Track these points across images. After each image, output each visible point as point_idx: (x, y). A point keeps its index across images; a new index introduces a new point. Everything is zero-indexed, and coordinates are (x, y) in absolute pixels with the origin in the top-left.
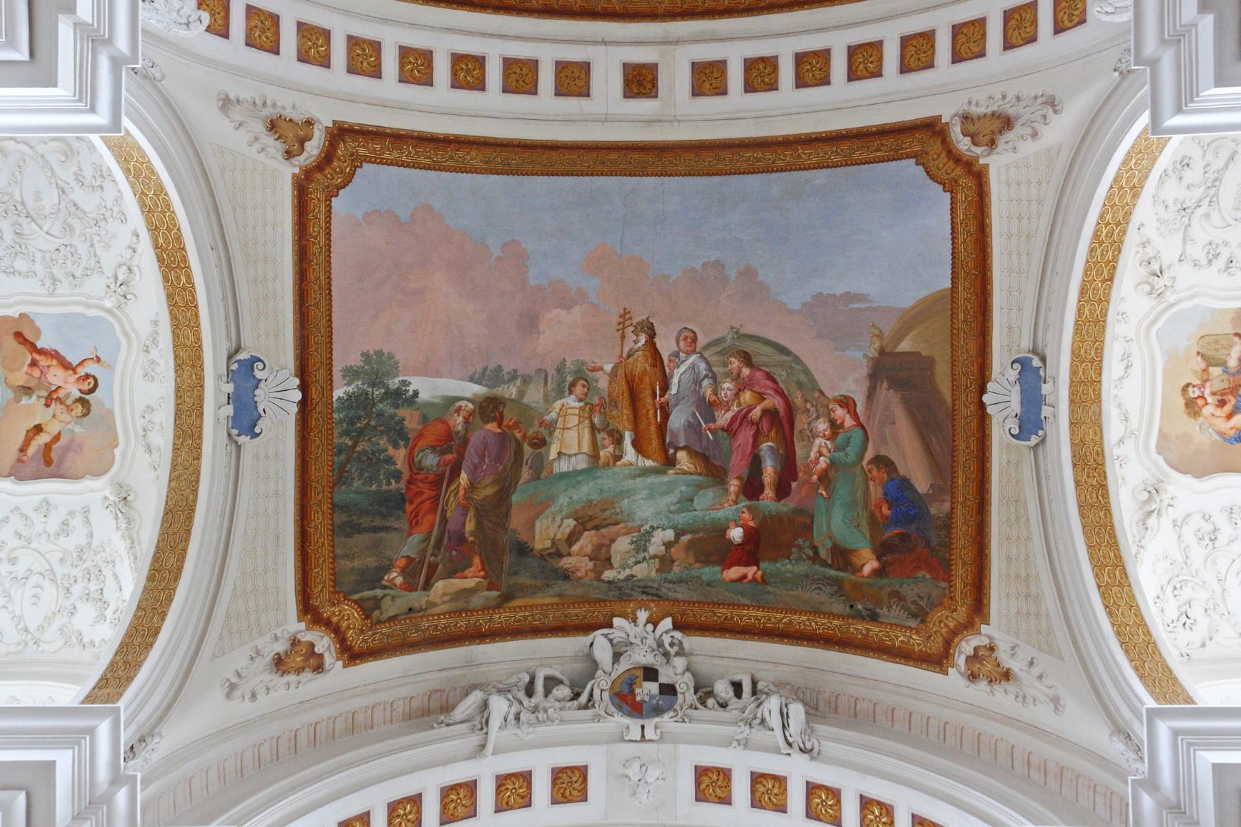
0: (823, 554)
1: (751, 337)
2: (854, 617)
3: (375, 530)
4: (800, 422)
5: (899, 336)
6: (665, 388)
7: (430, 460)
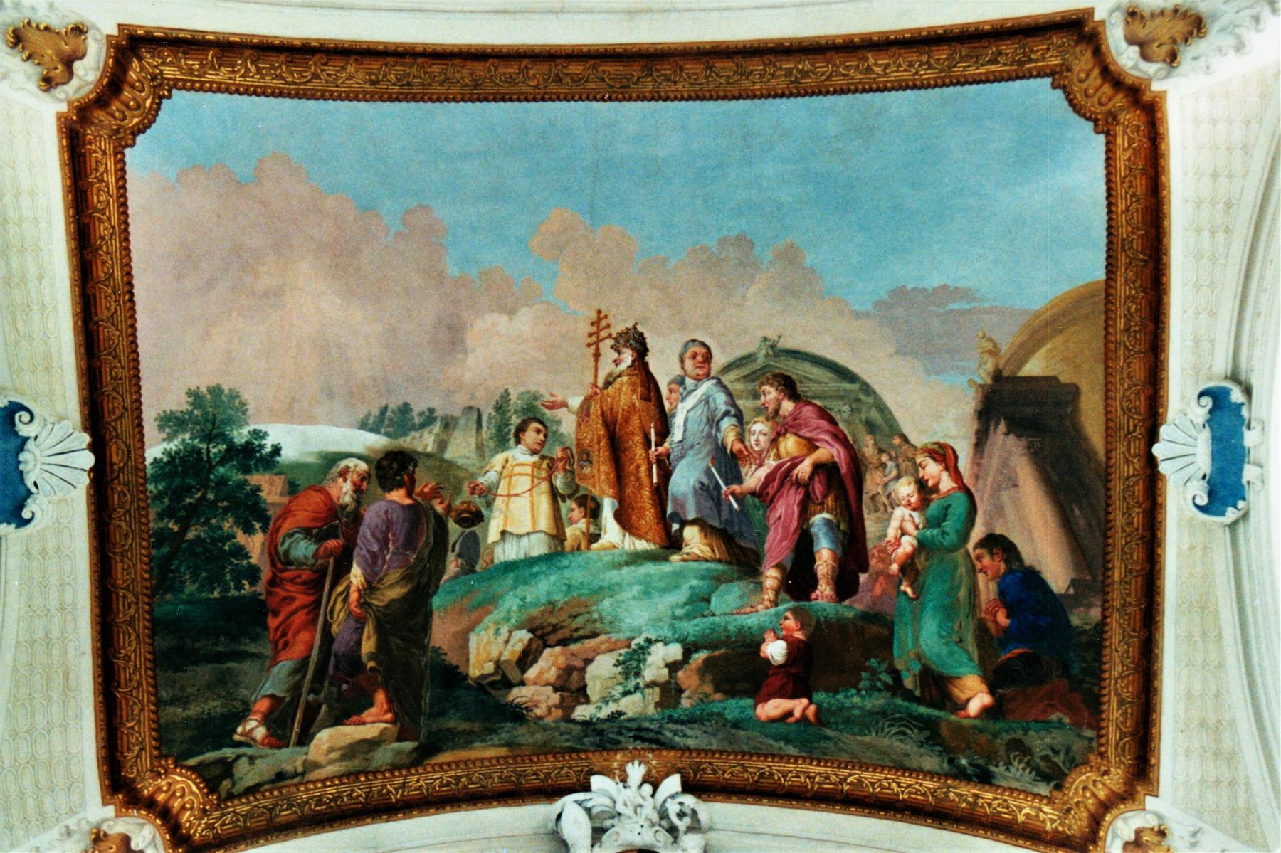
0: (908, 682)
1: (795, 354)
2: (955, 777)
3: (219, 658)
4: (873, 482)
5: (1026, 350)
6: (664, 432)
7: (303, 549)
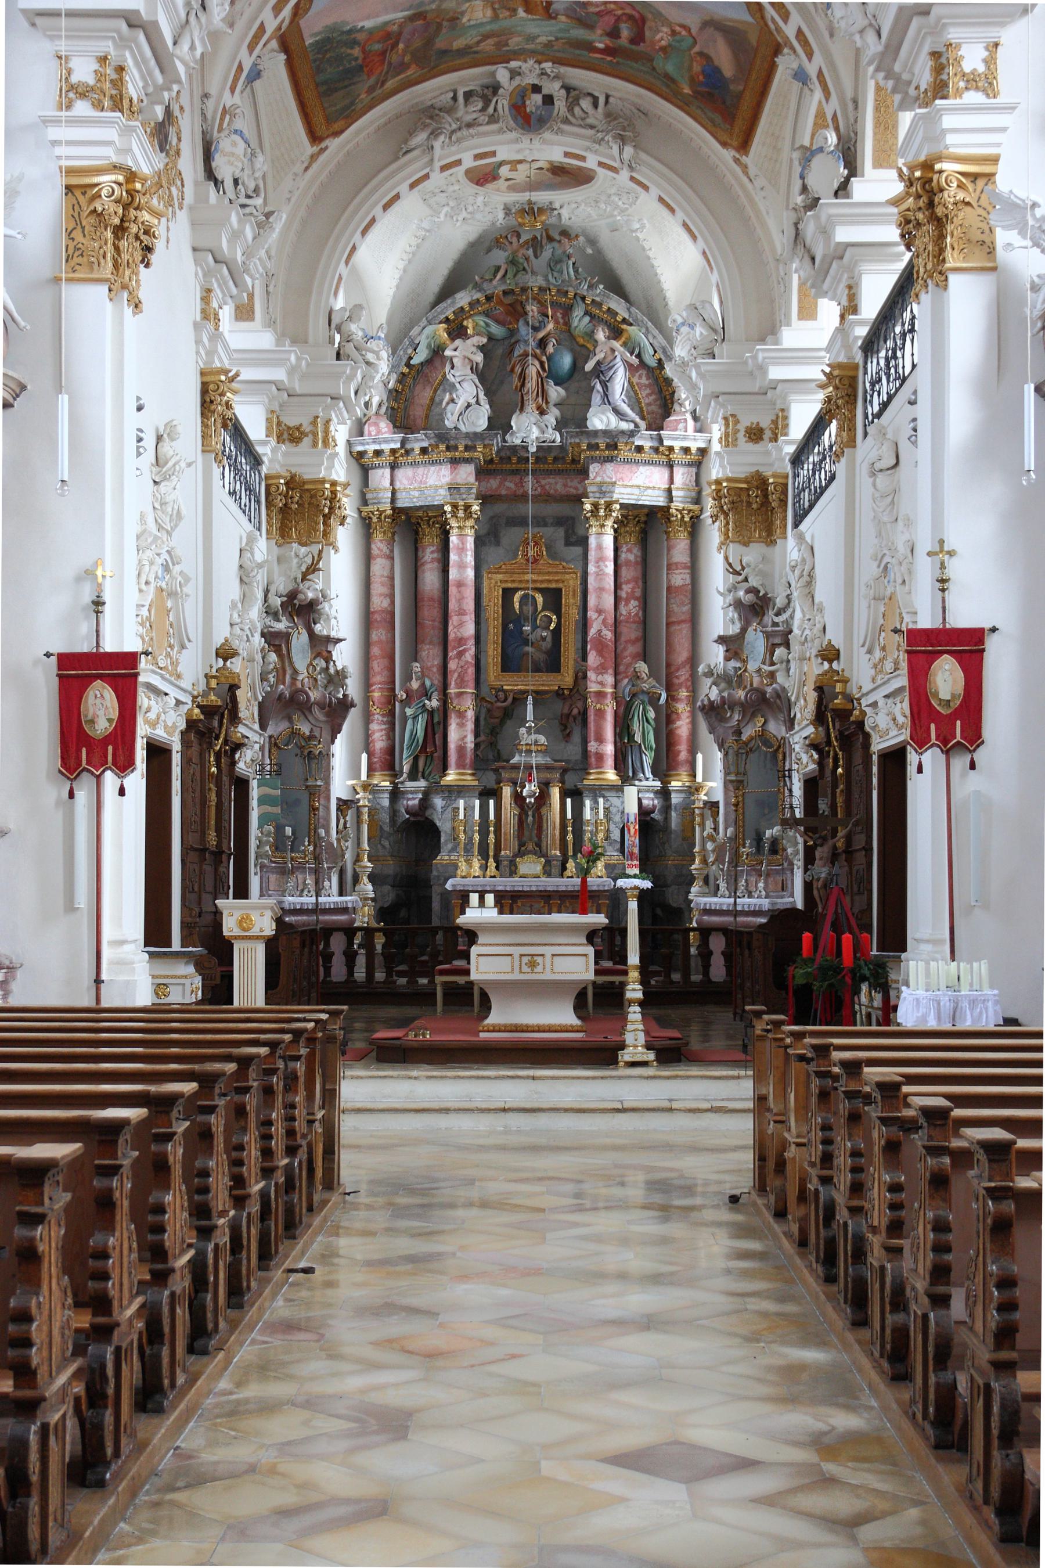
3: (346, 87)
